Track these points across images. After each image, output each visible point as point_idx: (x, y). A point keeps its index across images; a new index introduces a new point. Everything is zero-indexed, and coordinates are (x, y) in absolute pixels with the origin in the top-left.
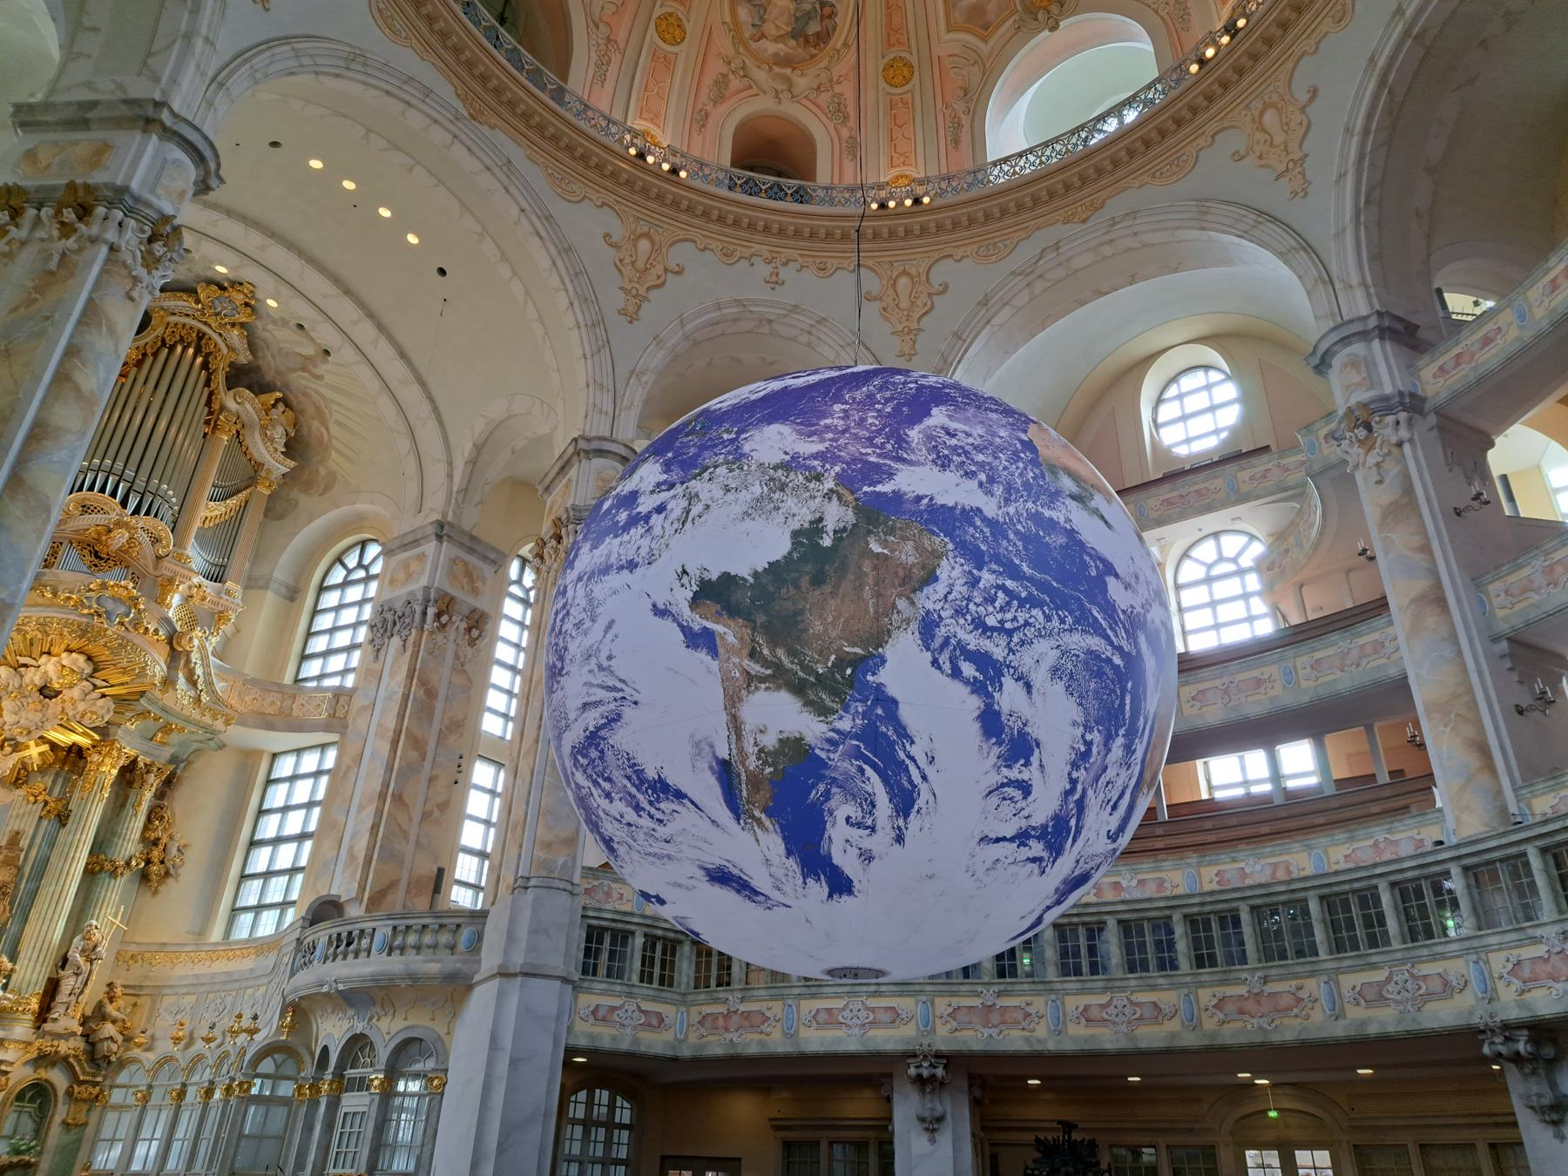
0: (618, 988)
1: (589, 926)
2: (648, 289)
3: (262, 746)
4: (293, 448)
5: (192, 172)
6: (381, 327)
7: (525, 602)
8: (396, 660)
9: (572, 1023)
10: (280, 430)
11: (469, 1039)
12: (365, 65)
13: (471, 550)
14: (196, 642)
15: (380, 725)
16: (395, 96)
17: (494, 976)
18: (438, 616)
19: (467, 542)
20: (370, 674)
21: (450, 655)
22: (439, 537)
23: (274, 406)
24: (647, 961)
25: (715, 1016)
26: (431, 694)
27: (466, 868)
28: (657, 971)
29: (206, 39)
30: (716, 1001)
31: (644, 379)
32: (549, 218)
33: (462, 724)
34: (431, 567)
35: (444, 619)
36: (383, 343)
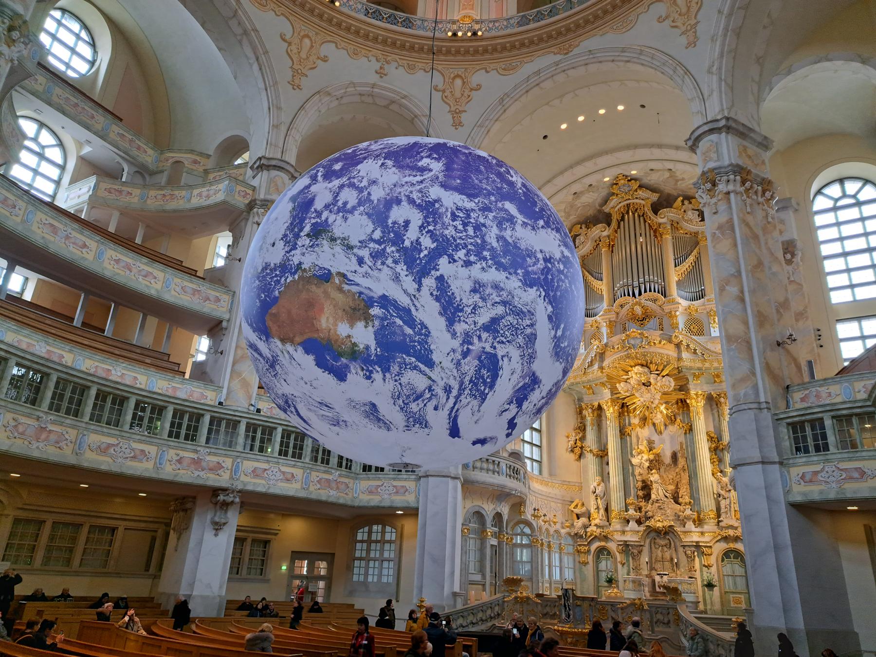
1: (788, 424)
10: (690, 213)
14: (681, 337)
23: (683, 204)
31: (715, 68)
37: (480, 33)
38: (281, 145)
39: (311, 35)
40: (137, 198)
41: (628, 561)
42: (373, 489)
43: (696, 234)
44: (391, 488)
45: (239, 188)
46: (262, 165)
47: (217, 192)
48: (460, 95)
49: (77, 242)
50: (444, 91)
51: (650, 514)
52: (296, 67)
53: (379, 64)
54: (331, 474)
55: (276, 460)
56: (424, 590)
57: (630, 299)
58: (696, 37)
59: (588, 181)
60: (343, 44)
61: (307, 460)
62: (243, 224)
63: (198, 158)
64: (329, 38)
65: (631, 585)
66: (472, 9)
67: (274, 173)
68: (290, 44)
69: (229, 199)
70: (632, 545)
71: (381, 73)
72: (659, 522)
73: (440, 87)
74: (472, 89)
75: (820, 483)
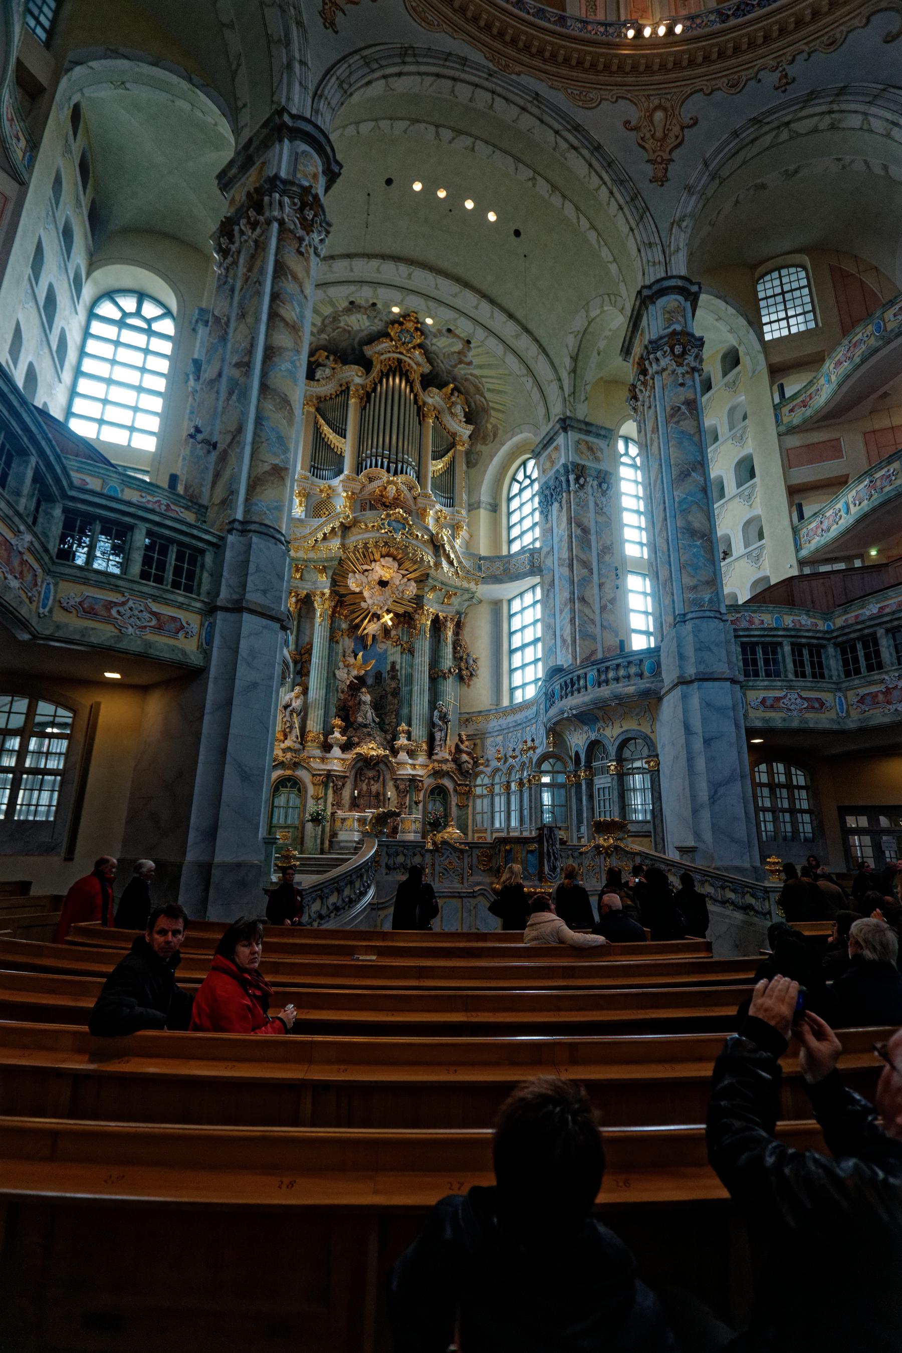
0: (779, 684)
2: (670, 152)
3: (501, 597)
4: (469, 418)
6: (492, 302)
7: (634, 466)
8: (558, 516)
9: (746, 711)
10: (459, 407)
11: (667, 729)
12: (415, 55)
13: (588, 433)
15: (559, 559)
16: (444, 77)
17: (675, 686)
18: (577, 480)
19: (584, 427)
20: (548, 532)
21: (591, 505)
22: (565, 429)
23: (452, 394)
24: (799, 664)
25: (874, 696)
26: (585, 531)
27: (638, 621)
28: (808, 670)
29: (301, 62)
30: (871, 683)
31: (684, 224)
32: (577, 128)
33: (610, 548)
34: (565, 450)
35: (582, 481)
36: (498, 313)
41: (326, 794)
42: (99, 608)
43: (454, 435)
44: (146, 615)
51: (356, 740)
54: (17, 532)
56: (221, 834)
57: (385, 476)
58: (665, 175)
59: (383, 293)
65: (356, 824)
70: (336, 776)
72: (372, 749)
75: (780, 709)
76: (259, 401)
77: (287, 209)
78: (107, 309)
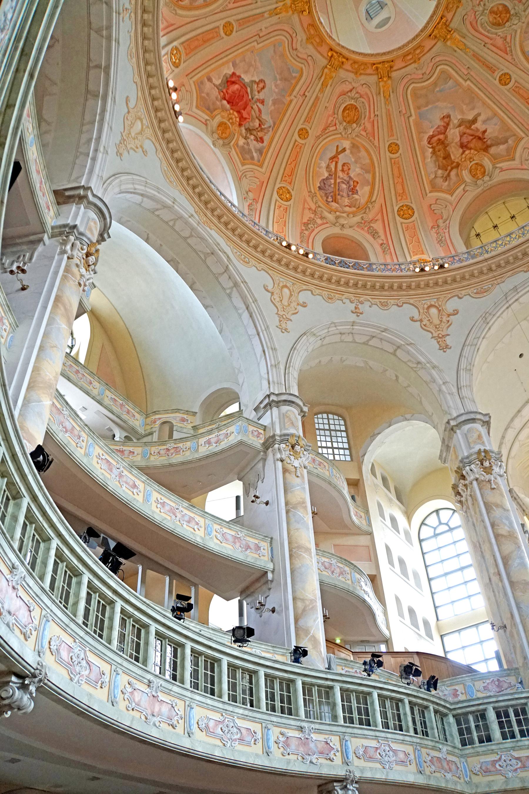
5: (477, 426)
37: (446, 265)
38: (284, 383)
39: (288, 285)
40: (140, 456)
45: (251, 428)
46: (271, 403)
47: (227, 436)
48: (438, 322)
49: (129, 480)
50: (421, 321)
52: (281, 313)
53: (353, 305)
54: (440, 750)
55: (383, 735)
60: (318, 291)
61: (412, 733)
62: (260, 465)
63: (185, 416)
64: (304, 287)
66: (423, 254)
67: (285, 408)
68: (272, 294)
69: (245, 439)
71: (357, 312)
73: (417, 317)
74: (449, 315)
76: (513, 593)
77: (475, 470)
78: (426, 532)
